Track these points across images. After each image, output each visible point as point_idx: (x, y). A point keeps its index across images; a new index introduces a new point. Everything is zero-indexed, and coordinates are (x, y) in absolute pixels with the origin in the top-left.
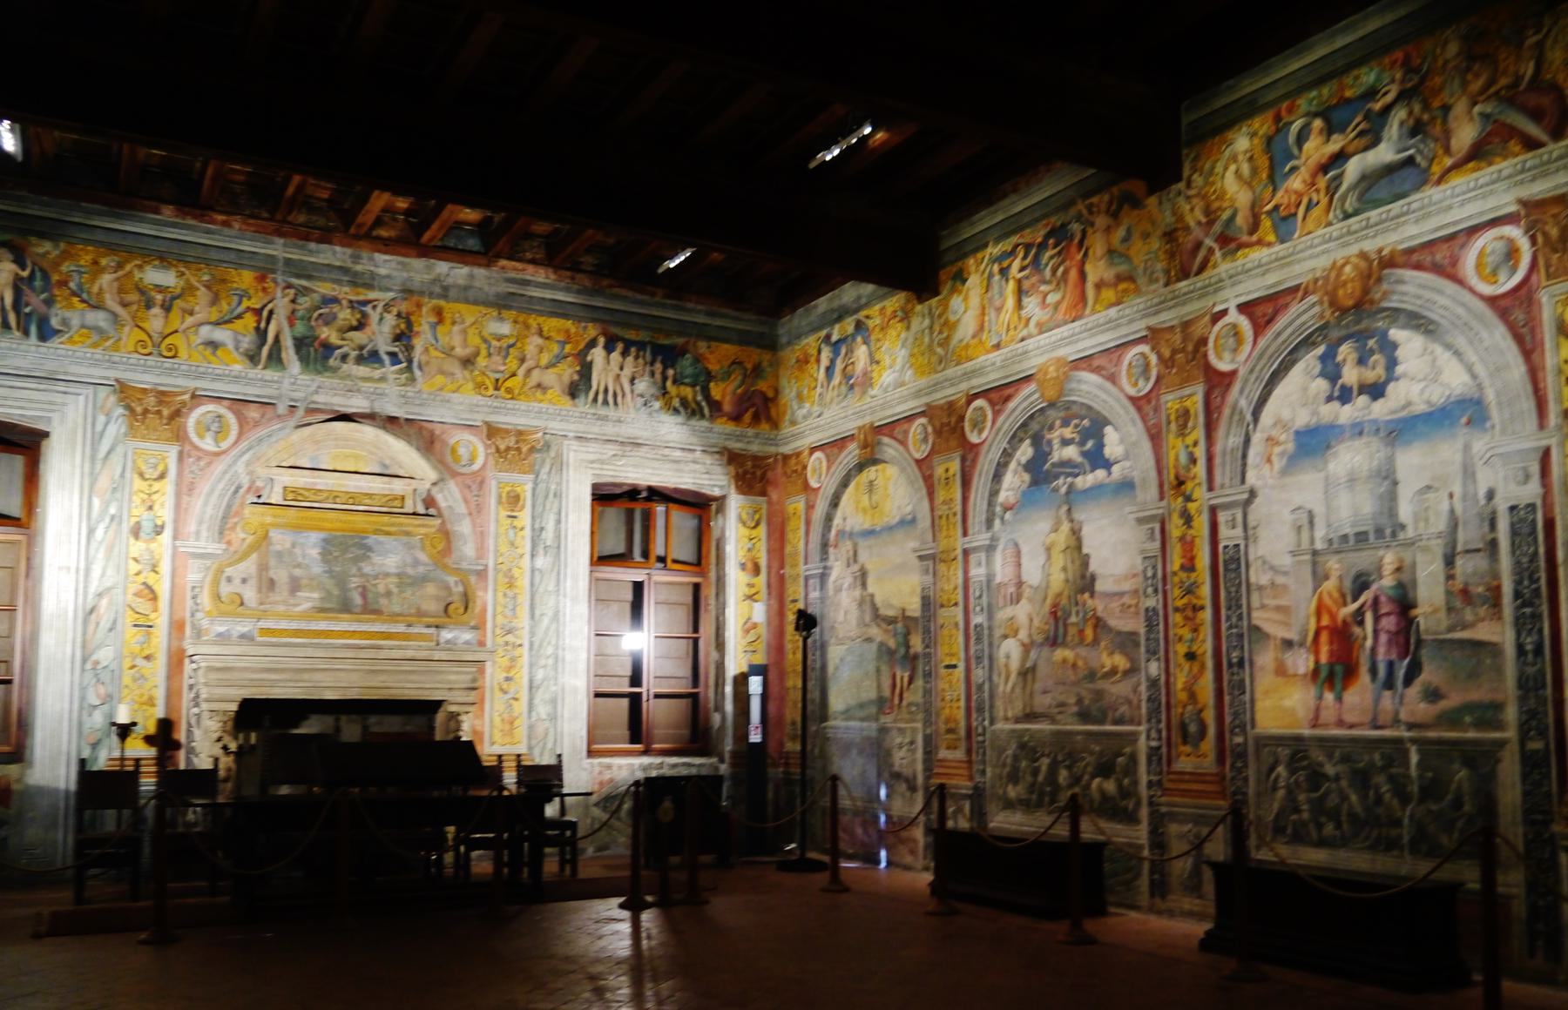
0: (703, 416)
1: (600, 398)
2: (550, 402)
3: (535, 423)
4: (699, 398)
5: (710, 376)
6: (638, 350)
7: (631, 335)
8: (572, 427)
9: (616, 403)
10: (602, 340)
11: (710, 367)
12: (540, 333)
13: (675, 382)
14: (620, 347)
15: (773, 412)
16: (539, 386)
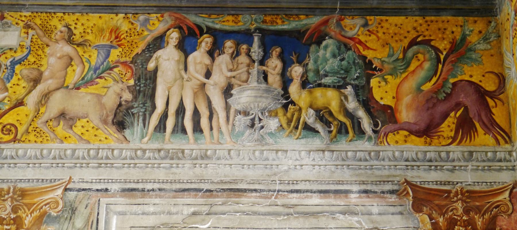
0: (360, 132)
1: (170, 123)
2: (81, 138)
3: (50, 174)
4: (352, 104)
5: (369, 68)
6: (238, 45)
7: (226, 23)
8: (115, 174)
9: (197, 129)
10: (174, 36)
11: (370, 55)
12: (70, 41)
13: (304, 84)
14: (206, 41)
15: (498, 114)
16: (62, 115)
